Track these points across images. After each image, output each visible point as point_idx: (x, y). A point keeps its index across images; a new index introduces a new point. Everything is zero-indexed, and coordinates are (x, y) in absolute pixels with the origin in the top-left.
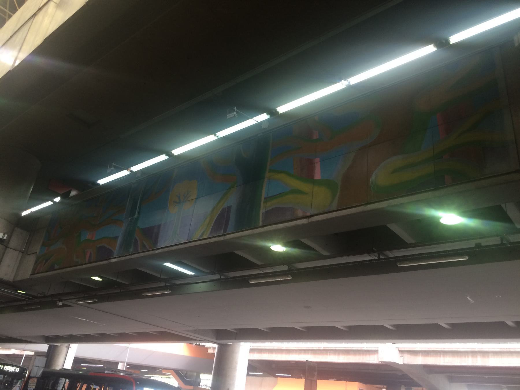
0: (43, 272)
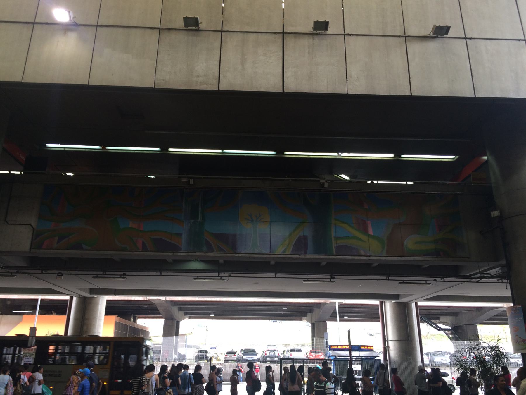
0: (56, 249)
